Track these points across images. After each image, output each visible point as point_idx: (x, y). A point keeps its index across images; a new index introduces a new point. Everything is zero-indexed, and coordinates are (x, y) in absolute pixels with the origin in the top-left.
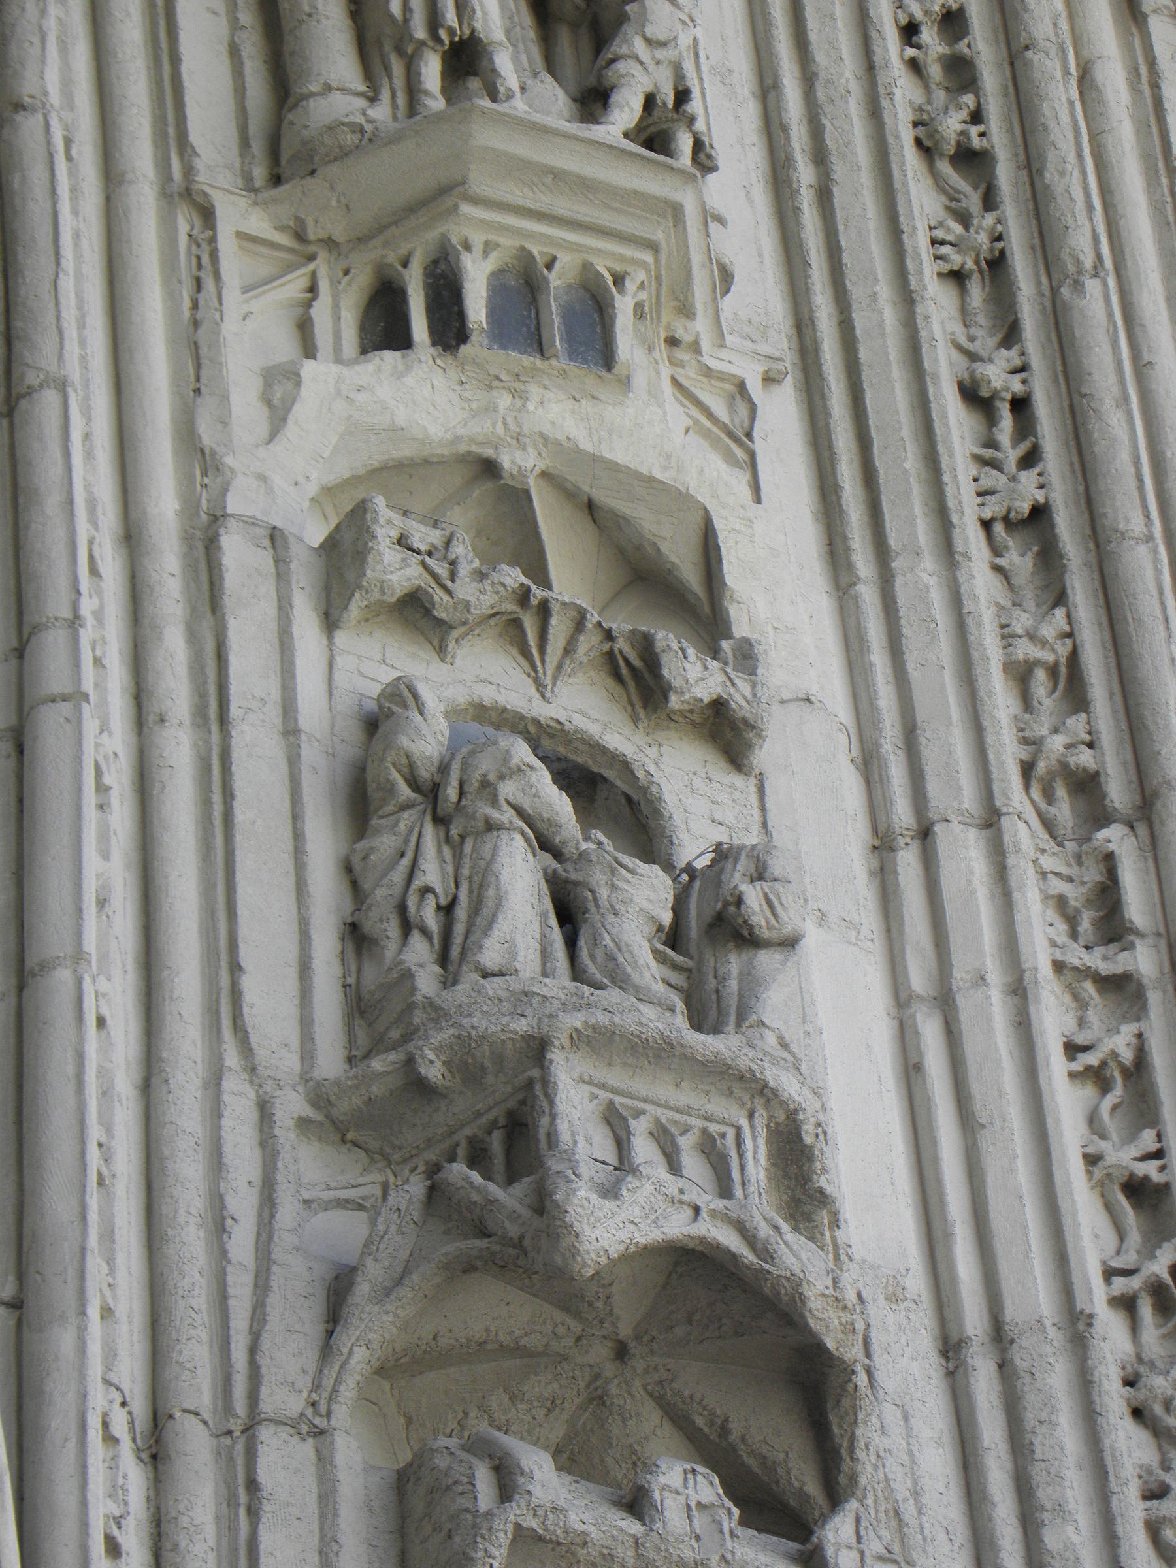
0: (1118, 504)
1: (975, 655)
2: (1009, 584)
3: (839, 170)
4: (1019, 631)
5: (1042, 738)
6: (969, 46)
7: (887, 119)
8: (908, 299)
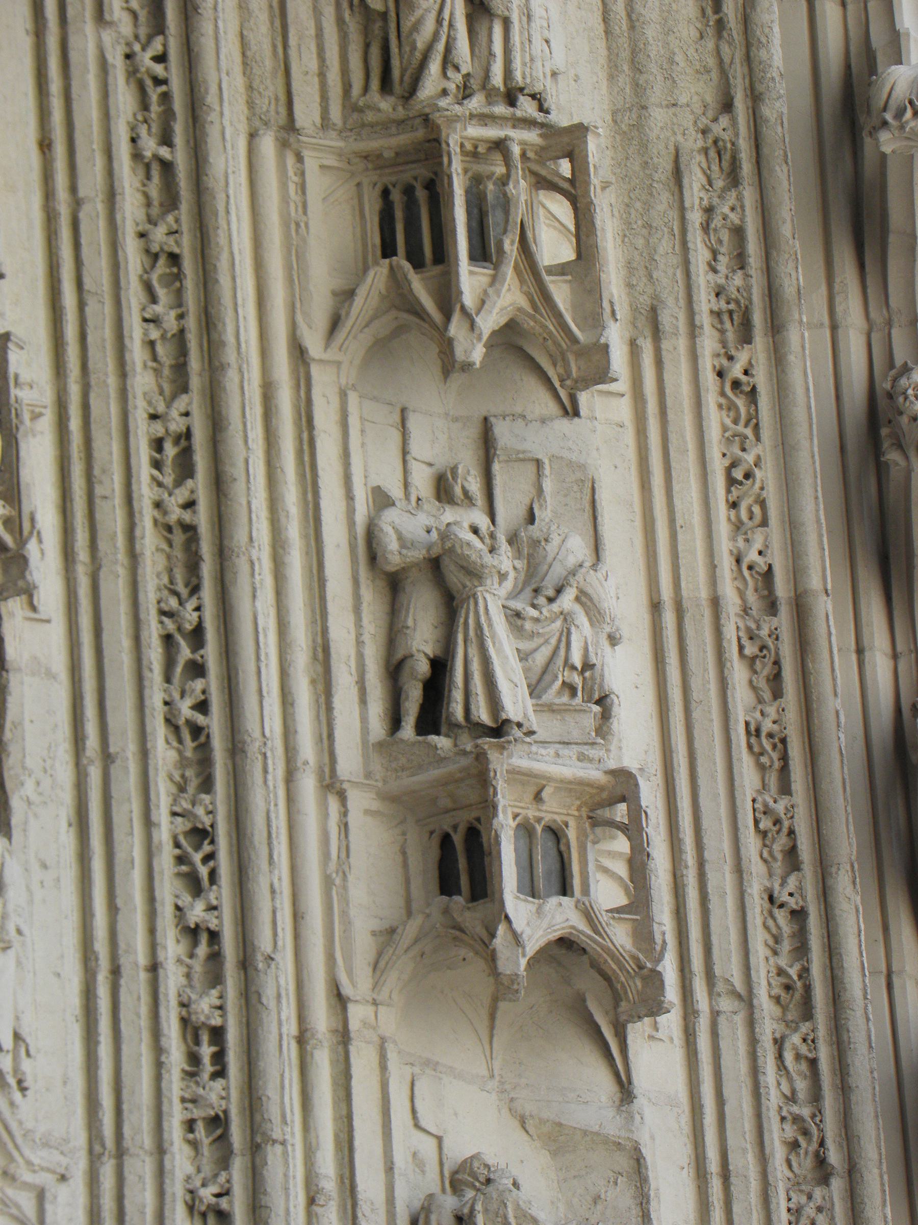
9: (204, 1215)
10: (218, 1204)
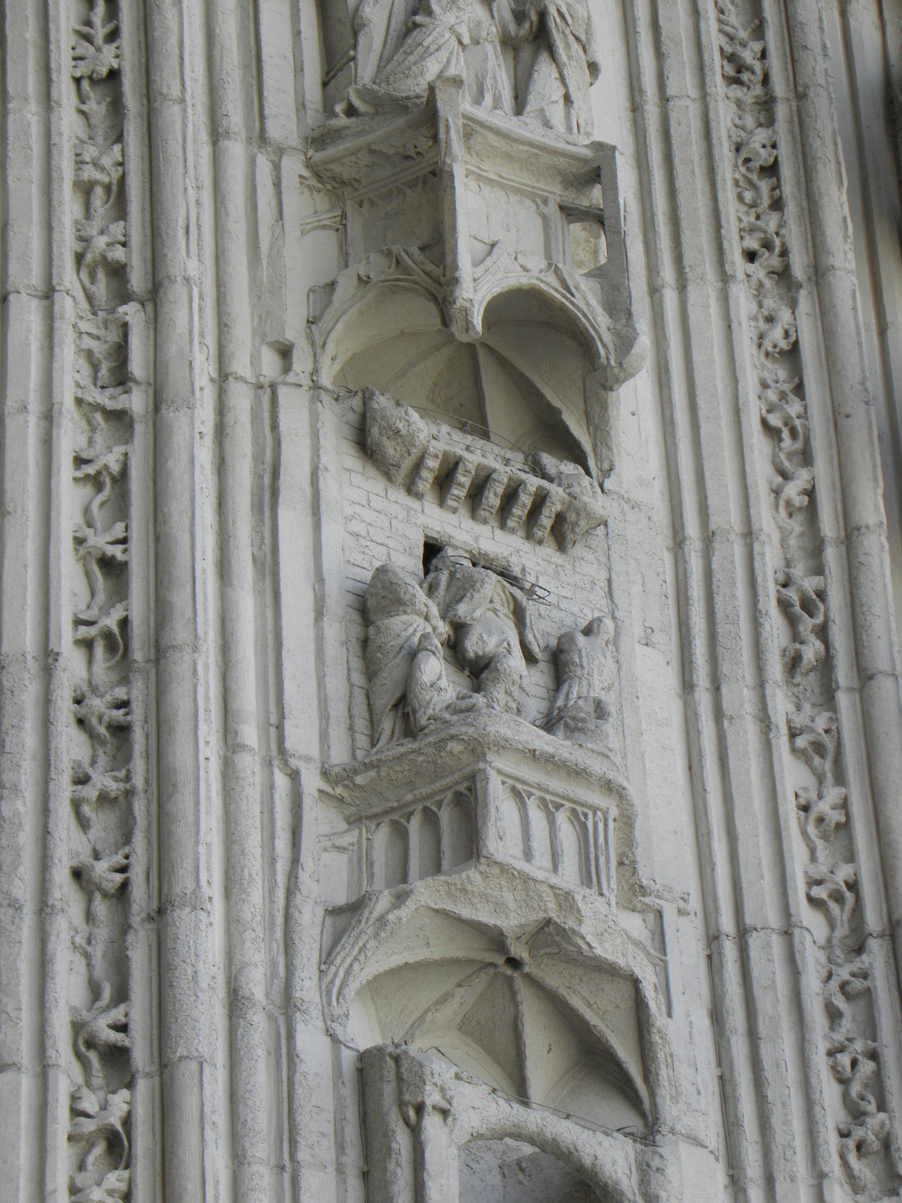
0: (165, 74)
1: (55, 175)
2: (88, 122)
4: (88, 159)
5: (92, 237)
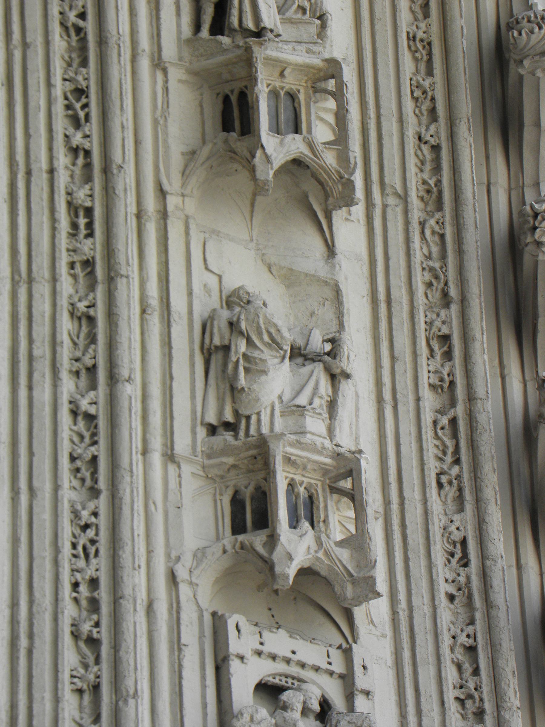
3: (37, 642)
6: (98, 594)
7: (60, 622)
8: (57, 700)
9: (79, 318)
10: (88, 312)
